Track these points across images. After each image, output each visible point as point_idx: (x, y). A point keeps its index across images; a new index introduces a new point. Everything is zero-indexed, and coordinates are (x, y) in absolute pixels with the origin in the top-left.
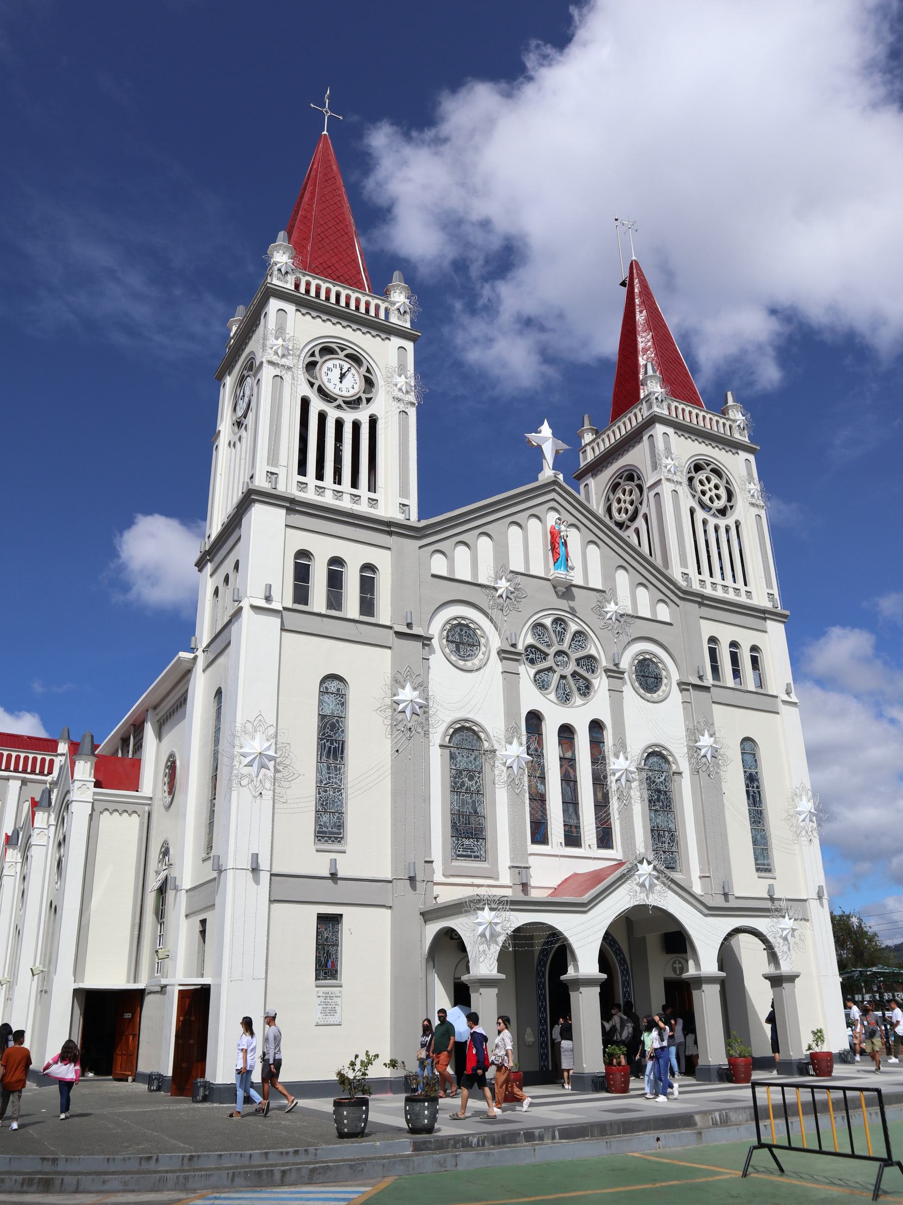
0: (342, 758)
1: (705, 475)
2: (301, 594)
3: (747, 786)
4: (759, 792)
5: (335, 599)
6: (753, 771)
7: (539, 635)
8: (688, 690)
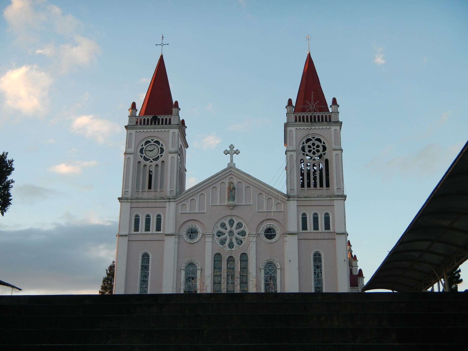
0: (148, 277)
1: (312, 143)
2: (137, 229)
3: (315, 270)
4: (321, 273)
5: (147, 229)
6: (319, 264)
7: (223, 226)
8: (287, 236)
